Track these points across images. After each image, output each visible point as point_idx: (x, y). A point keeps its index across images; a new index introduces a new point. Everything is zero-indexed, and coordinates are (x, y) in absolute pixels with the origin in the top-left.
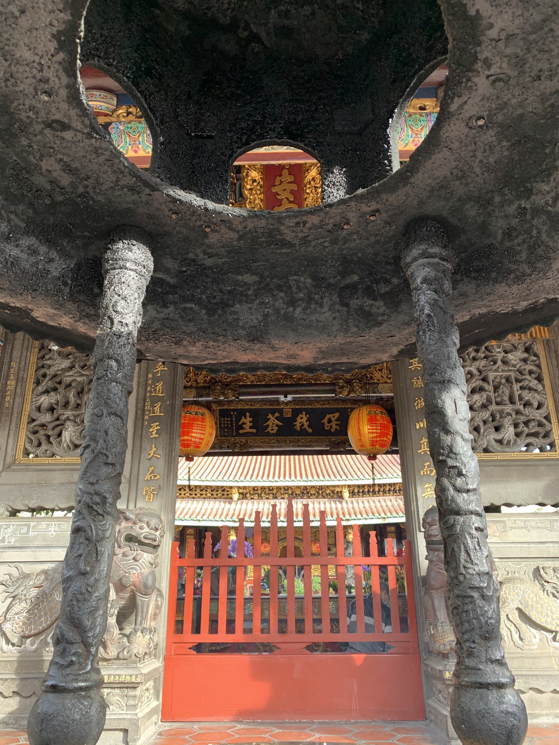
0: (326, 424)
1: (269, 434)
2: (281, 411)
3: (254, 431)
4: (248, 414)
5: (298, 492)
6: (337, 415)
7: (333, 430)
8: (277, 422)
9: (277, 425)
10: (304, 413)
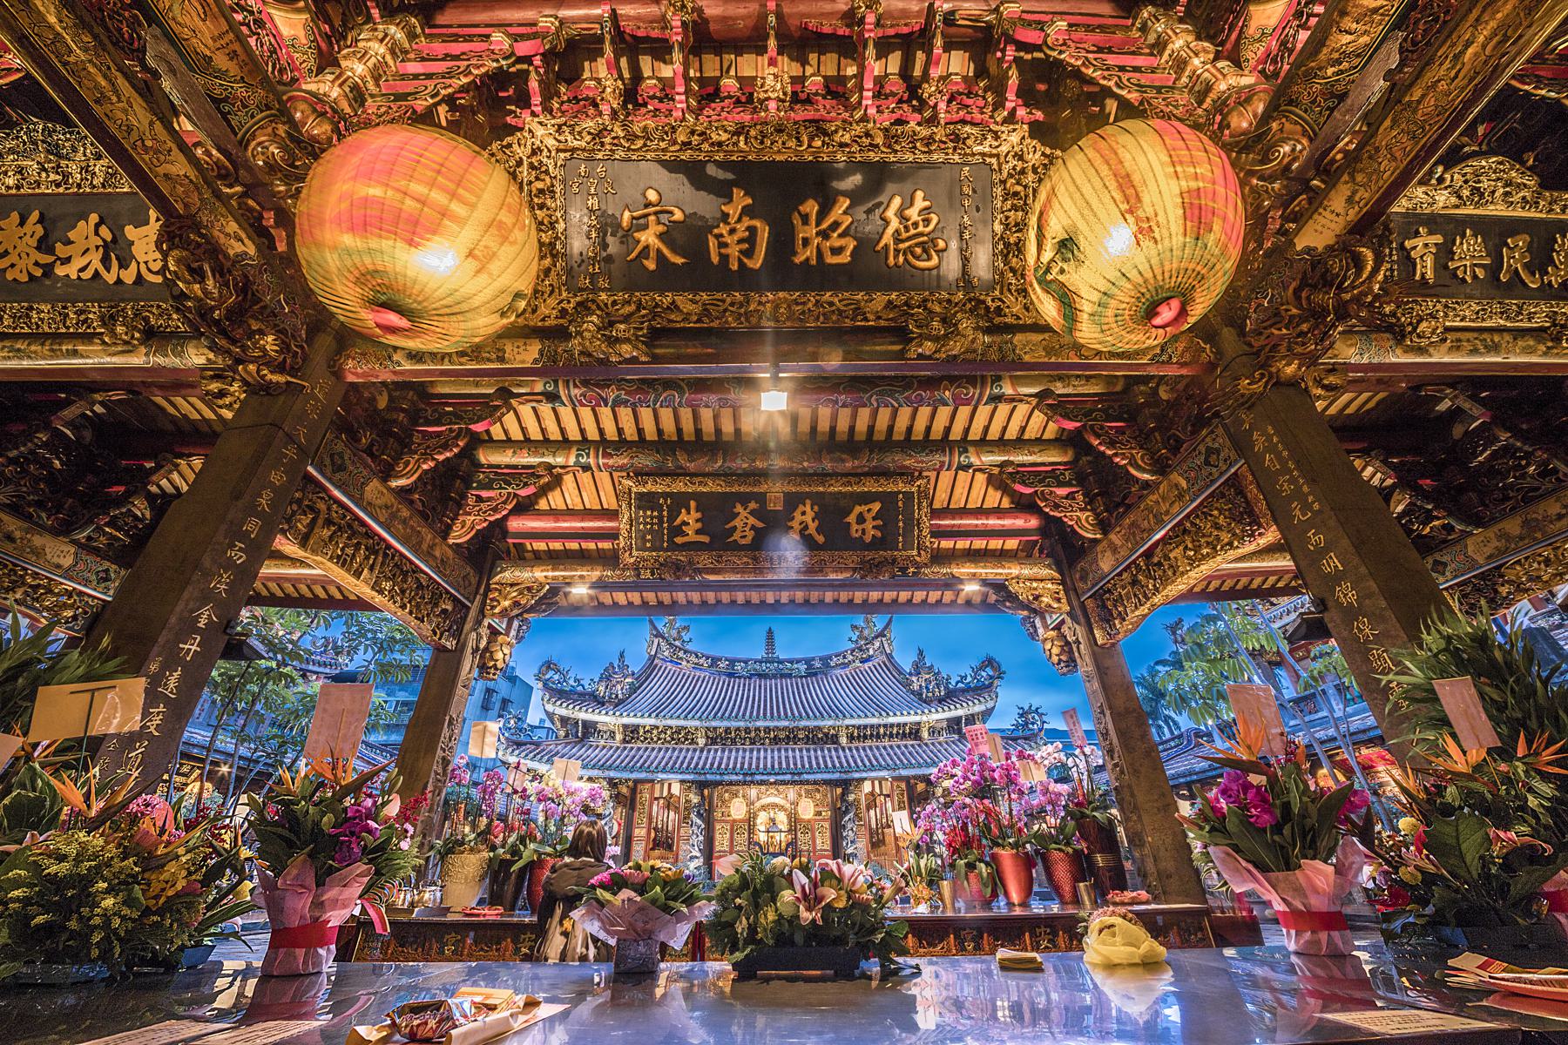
0: (855, 527)
1: (736, 547)
2: (761, 498)
3: (705, 539)
4: (693, 504)
5: (782, 735)
6: (876, 506)
7: (868, 539)
8: (752, 521)
9: (753, 528)
10: (808, 502)
